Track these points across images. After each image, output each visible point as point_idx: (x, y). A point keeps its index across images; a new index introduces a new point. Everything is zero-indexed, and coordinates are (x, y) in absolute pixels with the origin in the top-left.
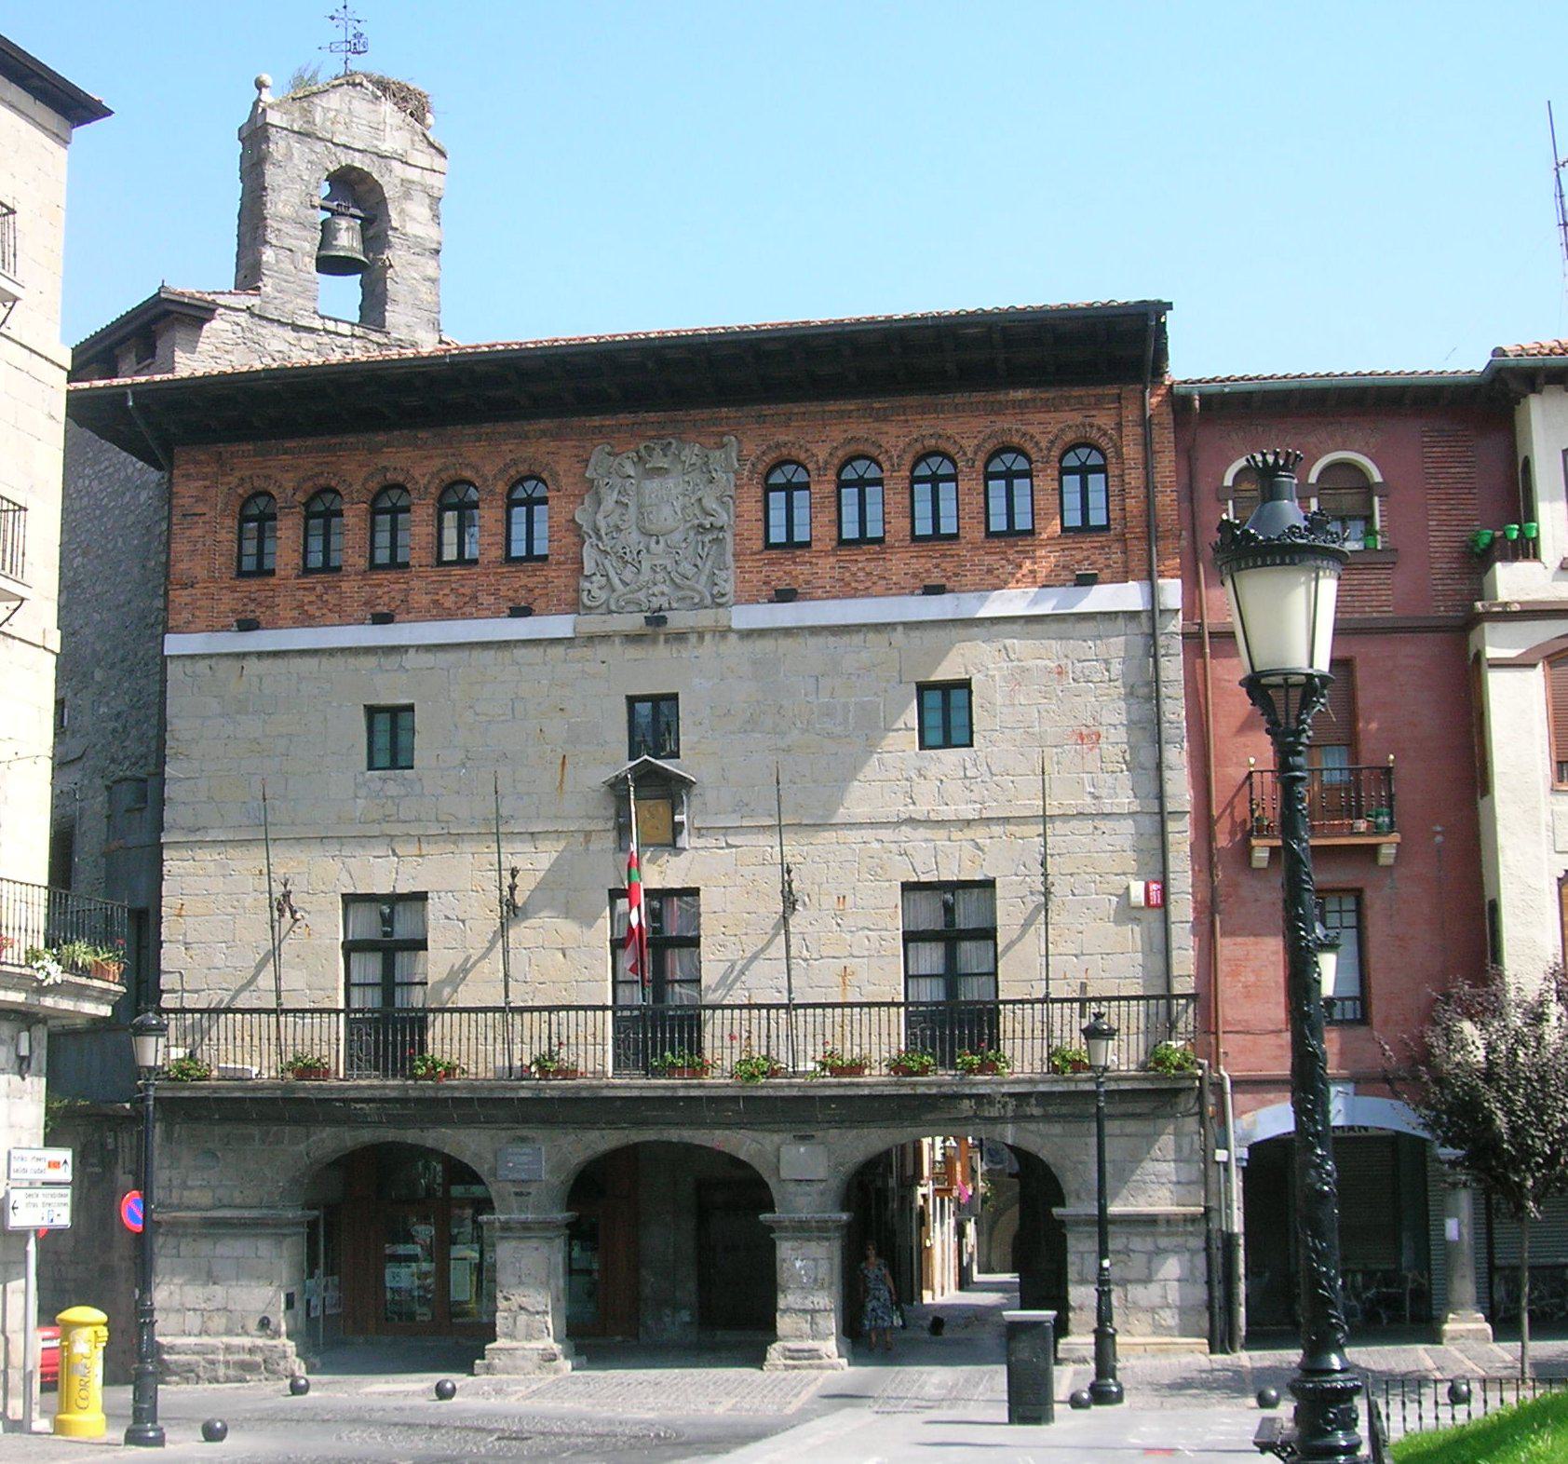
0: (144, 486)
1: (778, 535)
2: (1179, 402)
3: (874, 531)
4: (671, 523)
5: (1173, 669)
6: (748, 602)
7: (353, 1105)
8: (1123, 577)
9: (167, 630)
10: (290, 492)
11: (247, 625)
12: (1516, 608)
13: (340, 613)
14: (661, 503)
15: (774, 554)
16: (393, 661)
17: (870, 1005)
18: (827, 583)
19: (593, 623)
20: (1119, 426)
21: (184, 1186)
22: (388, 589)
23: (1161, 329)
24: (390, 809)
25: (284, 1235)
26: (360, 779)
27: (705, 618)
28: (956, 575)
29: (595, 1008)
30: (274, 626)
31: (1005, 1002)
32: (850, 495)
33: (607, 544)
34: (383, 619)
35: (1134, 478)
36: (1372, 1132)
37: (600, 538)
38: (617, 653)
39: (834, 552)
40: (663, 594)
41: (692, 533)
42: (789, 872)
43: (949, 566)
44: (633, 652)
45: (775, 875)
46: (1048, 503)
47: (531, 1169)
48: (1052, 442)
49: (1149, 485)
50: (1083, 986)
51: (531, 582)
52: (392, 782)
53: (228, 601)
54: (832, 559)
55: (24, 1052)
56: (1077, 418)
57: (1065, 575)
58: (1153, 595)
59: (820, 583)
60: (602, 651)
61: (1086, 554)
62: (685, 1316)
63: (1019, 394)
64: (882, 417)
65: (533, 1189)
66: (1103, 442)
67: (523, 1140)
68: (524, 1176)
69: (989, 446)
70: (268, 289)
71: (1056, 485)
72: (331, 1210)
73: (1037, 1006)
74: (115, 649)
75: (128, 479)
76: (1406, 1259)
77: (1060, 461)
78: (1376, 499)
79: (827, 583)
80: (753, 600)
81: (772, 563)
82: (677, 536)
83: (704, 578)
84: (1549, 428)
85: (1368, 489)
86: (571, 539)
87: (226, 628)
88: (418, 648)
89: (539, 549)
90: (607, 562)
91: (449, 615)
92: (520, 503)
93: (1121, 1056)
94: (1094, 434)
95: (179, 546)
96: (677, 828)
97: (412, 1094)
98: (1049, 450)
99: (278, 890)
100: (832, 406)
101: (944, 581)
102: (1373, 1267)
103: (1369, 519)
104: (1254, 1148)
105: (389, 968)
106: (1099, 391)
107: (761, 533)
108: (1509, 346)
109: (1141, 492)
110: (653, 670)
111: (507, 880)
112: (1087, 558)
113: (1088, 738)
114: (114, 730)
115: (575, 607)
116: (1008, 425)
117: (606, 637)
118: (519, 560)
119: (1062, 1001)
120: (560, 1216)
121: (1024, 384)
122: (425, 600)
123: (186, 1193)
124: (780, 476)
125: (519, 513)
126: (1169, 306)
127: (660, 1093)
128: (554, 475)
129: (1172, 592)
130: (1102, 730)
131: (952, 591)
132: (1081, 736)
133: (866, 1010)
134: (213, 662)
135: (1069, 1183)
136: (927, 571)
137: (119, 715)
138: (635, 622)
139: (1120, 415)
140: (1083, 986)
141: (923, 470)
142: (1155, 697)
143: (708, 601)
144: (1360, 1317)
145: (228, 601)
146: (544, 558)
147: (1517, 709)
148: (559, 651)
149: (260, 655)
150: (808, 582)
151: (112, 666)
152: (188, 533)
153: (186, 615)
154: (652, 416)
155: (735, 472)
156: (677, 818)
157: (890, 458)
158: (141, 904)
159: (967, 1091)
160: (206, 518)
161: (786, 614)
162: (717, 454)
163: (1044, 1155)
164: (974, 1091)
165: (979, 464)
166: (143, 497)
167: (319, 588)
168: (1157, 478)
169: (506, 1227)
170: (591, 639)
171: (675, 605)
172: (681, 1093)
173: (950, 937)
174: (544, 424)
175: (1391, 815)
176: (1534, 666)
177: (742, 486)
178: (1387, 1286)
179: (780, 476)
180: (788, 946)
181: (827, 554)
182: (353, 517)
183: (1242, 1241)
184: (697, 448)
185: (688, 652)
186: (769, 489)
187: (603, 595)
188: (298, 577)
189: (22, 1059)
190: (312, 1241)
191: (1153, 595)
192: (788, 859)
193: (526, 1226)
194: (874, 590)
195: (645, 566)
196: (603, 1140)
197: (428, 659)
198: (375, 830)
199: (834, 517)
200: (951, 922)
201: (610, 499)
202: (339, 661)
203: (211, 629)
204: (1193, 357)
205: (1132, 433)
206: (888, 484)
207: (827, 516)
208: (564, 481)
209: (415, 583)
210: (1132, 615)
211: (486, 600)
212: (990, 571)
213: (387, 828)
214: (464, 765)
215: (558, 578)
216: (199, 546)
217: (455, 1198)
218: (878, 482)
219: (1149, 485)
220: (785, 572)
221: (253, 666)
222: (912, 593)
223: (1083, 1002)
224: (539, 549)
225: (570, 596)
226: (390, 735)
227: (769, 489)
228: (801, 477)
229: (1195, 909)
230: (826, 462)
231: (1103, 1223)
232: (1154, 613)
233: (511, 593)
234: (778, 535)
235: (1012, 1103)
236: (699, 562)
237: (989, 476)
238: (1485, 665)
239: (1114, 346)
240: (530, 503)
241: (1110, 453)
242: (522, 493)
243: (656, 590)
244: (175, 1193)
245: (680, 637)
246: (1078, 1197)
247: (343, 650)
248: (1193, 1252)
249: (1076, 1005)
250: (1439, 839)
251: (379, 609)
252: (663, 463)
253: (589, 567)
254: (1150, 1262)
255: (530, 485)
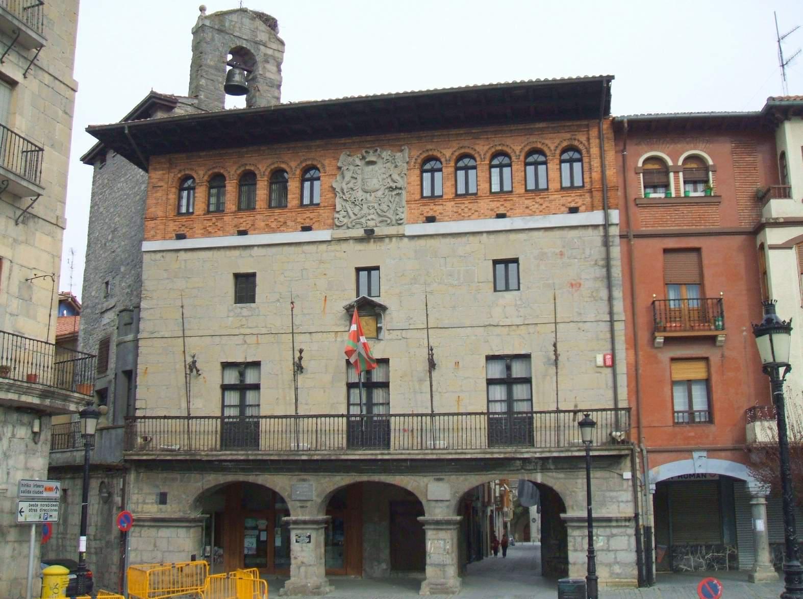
0: (143, 182)
1: (427, 193)
2: (617, 125)
3: (472, 190)
4: (377, 186)
5: (616, 251)
6: (413, 223)
7: (224, 464)
8: (592, 208)
9: (145, 239)
10: (202, 176)
11: (180, 237)
12: (782, 220)
13: (224, 231)
14: (371, 179)
15: (425, 201)
16: (247, 252)
17: (470, 414)
18: (450, 213)
19: (340, 233)
20: (588, 139)
21: (144, 503)
22: (245, 220)
23: (608, 89)
24: (244, 321)
25: (190, 527)
26: (230, 308)
27: (392, 230)
28: (511, 209)
29: (338, 416)
30: (192, 237)
31: (536, 413)
32: (461, 174)
33: (347, 196)
34: (243, 233)
35: (596, 163)
36: (708, 478)
37: (344, 194)
38: (351, 246)
39: (453, 199)
40: (373, 219)
41: (387, 191)
42: (432, 350)
43: (508, 204)
44: (360, 246)
45: (425, 353)
46: (556, 173)
47: (305, 496)
48: (557, 147)
49: (603, 166)
50: (576, 406)
51: (312, 215)
52: (245, 309)
53: (172, 226)
54: (453, 203)
55: (36, 429)
56: (568, 136)
57: (563, 209)
58: (606, 217)
59: (448, 214)
60: (344, 246)
61: (573, 199)
62: (384, 566)
63: (542, 125)
64: (476, 137)
65: (309, 504)
66: (581, 147)
67: (304, 480)
68: (304, 498)
69: (527, 149)
70: (202, 97)
71: (558, 167)
72: (218, 516)
73: (553, 415)
74: (129, 256)
75: (137, 180)
76: (726, 540)
77: (560, 156)
78: (710, 173)
79: (450, 213)
80: (415, 222)
81: (424, 205)
82: (379, 194)
83: (391, 211)
84: (792, 135)
85: (706, 169)
86: (331, 195)
87: (170, 238)
88: (258, 246)
89: (316, 201)
90: (347, 206)
91: (273, 231)
92: (307, 180)
93: (597, 436)
94: (576, 143)
95: (151, 201)
96: (379, 330)
97: (251, 458)
98: (555, 150)
99: (189, 360)
100: (453, 132)
101: (505, 212)
102: (710, 543)
103: (706, 182)
104: (659, 484)
105: (243, 398)
106: (579, 123)
107: (419, 190)
108: (775, 95)
109: (599, 169)
110: (368, 255)
111: (297, 355)
112: (574, 200)
113: (575, 285)
114: (127, 293)
115: (334, 226)
116: (536, 141)
117: (346, 240)
118: (307, 205)
119: (565, 412)
120: (322, 517)
121: (544, 120)
122: (263, 224)
123: (145, 506)
124: (429, 164)
125: (307, 184)
126: (612, 77)
127: (369, 457)
128: (323, 166)
129: (615, 216)
130: (582, 282)
131: (509, 217)
132: (572, 285)
133: (469, 416)
134: (164, 254)
135: (568, 502)
136: (498, 207)
137: (129, 286)
138: (360, 232)
139: (588, 134)
140: (576, 406)
141: (496, 162)
142: (608, 267)
143: (394, 222)
144: (705, 567)
145: (172, 226)
146: (318, 205)
147: (783, 270)
148: (323, 247)
149: (186, 250)
150: (441, 213)
151: (128, 264)
152: (155, 195)
153: (152, 233)
154: (369, 138)
155: (407, 163)
156: (379, 325)
157: (480, 155)
158: (128, 368)
159: (519, 456)
160: (163, 188)
161: (431, 228)
162: (398, 154)
163: (556, 488)
164: (522, 456)
165: (522, 158)
166: (142, 188)
167: (214, 219)
168: (607, 163)
169: (296, 522)
170: (340, 240)
171: (378, 225)
172: (379, 457)
173: (508, 382)
174: (318, 142)
175: (723, 321)
176: (791, 248)
177: (411, 169)
178: (718, 552)
179: (429, 164)
180: (431, 386)
181: (450, 200)
182: (231, 187)
183: (653, 530)
184: (389, 153)
185: (386, 245)
186: (423, 171)
187: (345, 220)
188: (204, 215)
189: (35, 433)
190: (208, 529)
191: (606, 217)
192: (431, 344)
193: (305, 522)
194: (473, 217)
195: (365, 206)
196: (342, 480)
197: (262, 251)
198: (236, 332)
199: (453, 182)
200: (510, 372)
201: (348, 175)
202: (222, 252)
203: (164, 238)
204: (622, 106)
205: (594, 142)
206: (479, 168)
207: (450, 183)
208: (327, 169)
209: (258, 217)
210: (596, 227)
211: (290, 223)
212: (527, 208)
213: (243, 331)
214: (278, 300)
215: (324, 213)
216: (160, 201)
217: (272, 507)
218: (474, 168)
219: (603, 166)
220: (429, 211)
221: (182, 255)
222: (491, 218)
223: (575, 412)
224: (316, 201)
225: (330, 221)
226: (245, 287)
227: (423, 171)
228: (438, 165)
229: (627, 367)
230: (450, 157)
231: (590, 521)
232: (606, 226)
233: (302, 221)
234: (427, 193)
235: (540, 462)
236: (390, 205)
237: (526, 164)
238: (766, 248)
239: (584, 100)
240: (312, 180)
241: (584, 152)
242: (309, 173)
243: (369, 217)
244: (140, 506)
245: (381, 238)
246: (573, 508)
247: (224, 248)
248: (629, 536)
249: (572, 414)
250: (745, 333)
251: (241, 229)
252: (374, 159)
253: (338, 208)
254: (608, 540)
255: (312, 172)
